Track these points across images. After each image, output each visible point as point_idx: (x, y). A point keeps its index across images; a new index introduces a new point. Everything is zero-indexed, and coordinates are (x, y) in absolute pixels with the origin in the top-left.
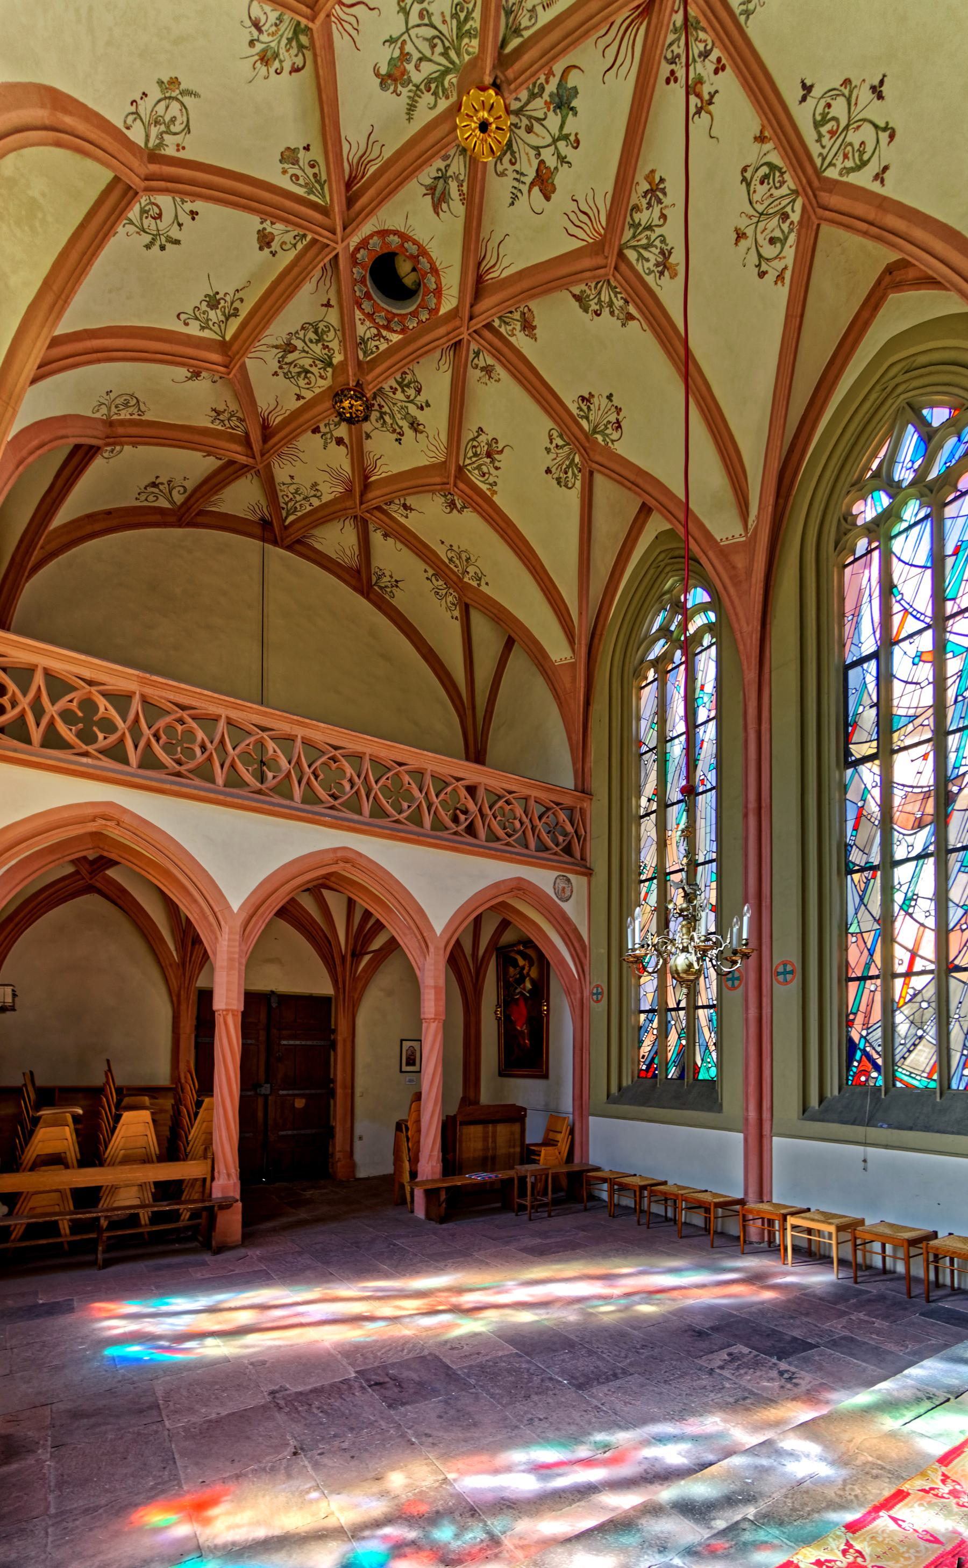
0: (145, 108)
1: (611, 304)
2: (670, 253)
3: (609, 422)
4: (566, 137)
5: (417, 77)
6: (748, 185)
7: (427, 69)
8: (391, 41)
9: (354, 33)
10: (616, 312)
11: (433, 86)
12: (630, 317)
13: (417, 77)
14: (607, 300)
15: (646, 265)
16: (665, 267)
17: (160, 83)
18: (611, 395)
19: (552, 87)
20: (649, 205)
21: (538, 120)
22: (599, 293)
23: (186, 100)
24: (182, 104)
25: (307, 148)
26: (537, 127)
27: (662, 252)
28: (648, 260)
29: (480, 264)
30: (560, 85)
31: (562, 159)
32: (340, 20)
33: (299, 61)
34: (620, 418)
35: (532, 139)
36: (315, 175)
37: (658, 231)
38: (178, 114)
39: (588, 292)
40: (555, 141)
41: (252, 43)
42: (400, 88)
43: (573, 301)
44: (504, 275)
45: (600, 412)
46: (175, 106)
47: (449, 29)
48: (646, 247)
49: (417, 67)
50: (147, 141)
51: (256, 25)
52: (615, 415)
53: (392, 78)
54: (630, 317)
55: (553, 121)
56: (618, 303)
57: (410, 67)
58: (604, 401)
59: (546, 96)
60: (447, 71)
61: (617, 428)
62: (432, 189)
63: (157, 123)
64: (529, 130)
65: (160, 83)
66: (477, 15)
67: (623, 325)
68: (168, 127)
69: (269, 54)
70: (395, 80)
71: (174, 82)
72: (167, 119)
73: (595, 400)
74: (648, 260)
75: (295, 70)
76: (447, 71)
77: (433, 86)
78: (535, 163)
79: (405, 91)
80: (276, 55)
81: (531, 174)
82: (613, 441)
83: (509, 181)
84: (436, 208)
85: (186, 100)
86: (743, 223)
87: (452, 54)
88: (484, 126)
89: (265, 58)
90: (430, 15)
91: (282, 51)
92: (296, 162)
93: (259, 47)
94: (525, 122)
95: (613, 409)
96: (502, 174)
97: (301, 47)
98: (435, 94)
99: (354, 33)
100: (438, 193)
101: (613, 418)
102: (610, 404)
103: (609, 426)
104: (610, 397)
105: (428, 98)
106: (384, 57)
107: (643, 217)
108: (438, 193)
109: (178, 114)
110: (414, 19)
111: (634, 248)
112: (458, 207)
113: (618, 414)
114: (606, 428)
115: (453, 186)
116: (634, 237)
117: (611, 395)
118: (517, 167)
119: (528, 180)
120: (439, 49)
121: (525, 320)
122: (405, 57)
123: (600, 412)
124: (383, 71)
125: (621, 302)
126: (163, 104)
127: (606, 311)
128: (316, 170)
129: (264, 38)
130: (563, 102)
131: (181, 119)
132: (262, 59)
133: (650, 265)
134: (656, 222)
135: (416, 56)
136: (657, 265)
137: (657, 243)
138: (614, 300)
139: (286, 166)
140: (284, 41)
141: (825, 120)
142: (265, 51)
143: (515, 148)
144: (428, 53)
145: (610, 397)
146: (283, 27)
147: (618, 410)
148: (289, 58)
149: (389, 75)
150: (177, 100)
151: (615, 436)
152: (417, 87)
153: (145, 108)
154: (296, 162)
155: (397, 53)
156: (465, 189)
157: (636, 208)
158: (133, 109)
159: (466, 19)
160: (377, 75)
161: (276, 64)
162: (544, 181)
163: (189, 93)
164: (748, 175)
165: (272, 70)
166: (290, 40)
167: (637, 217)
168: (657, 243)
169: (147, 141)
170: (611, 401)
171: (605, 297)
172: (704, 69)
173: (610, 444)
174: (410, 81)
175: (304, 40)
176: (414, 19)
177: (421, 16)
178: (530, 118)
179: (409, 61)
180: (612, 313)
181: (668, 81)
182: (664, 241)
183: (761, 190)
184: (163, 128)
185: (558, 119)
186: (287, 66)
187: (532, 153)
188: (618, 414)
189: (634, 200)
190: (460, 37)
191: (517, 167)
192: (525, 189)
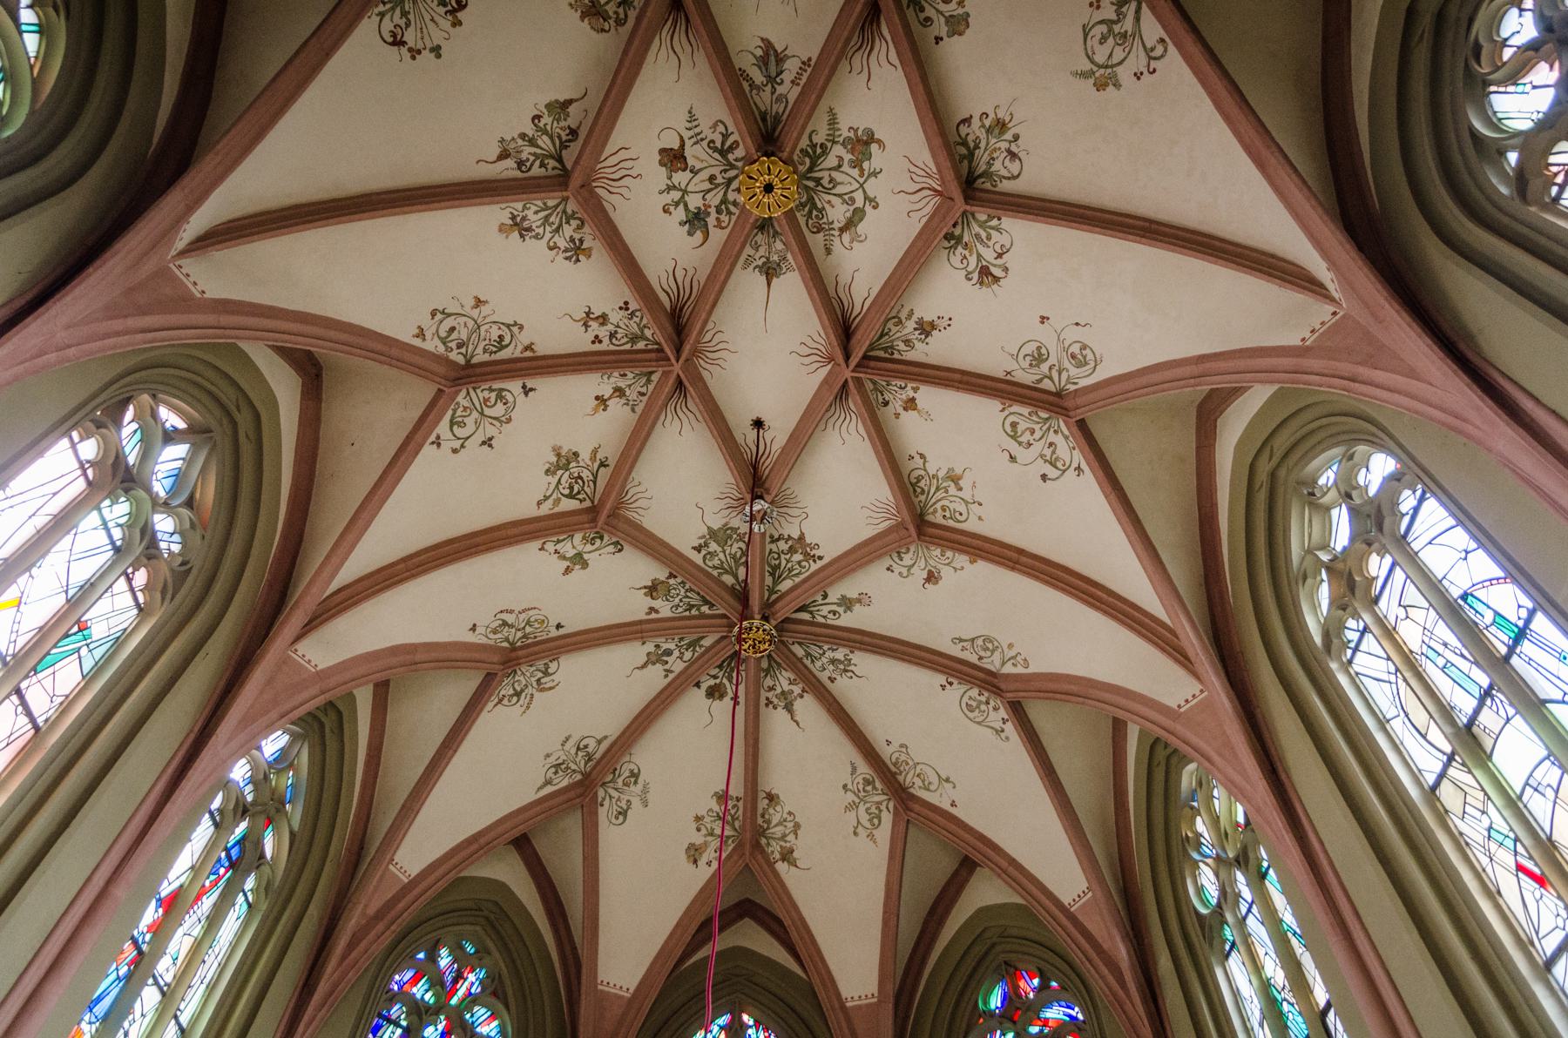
0: (1137, 60)
1: (532, 142)
2: (522, 236)
3: (408, 25)
4: (677, 204)
5: (838, 150)
6: (508, 326)
7: (831, 161)
8: (875, 174)
9: (913, 169)
10: (520, 142)
11: (819, 151)
12: (504, 155)
13: (838, 150)
14: (540, 142)
15: (534, 208)
16: (516, 224)
17: (1117, 85)
18: (439, 56)
19: (711, 221)
20: (572, 240)
21: (709, 191)
22: (551, 138)
23: (1088, 66)
24: (1092, 62)
25: (938, 39)
26: (707, 185)
27: (529, 229)
28: (536, 213)
29: (688, 21)
30: (706, 225)
31: (669, 188)
32: (930, 176)
33: (964, 130)
34: (404, 50)
35: (705, 175)
36: (922, 10)
37: (548, 236)
38: (1097, 47)
39: (563, 124)
40: (685, 192)
41: (1016, 138)
42: (852, 134)
43: (568, 97)
44: (657, 41)
45: (427, 18)
46: (1100, 58)
47: (822, 199)
48: (547, 218)
49: (841, 158)
50: (1138, 11)
51: (1013, 155)
52: (411, 44)
53: (863, 143)
54: (504, 155)
55: (694, 202)
56: (527, 152)
57: (847, 157)
58: (437, 37)
59: (713, 210)
60: (811, 170)
61: (394, 35)
62: (780, 60)
63: (1124, 35)
64: (712, 178)
65: (1117, 85)
66: (802, 221)
67: (502, 141)
68: (1110, 30)
69: (997, 131)
70: (858, 141)
71: (1100, 86)
72: (1111, 41)
73: (445, 24)
74: (536, 213)
75: (967, 121)
76: (811, 170)
77: (819, 151)
78: (691, 162)
79: (845, 133)
80: (989, 131)
81: (688, 152)
82: (382, 15)
83: (705, 126)
84: (768, 45)
85: (1088, 66)
86: (485, 310)
87: (811, 184)
88: (769, 188)
89: (1001, 126)
90: (845, 202)
91: (982, 134)
92: (950, 20)
93: (1008, 136)
94: (720, 180)
95: (420, 46)
96: (715, 126)
97: (964, 143)
98: (814, 146)
99: (913, 169)
100: (772, 58)
101: (410, 37)
102: (429, 45)
103: (402, 22)
104: (436, 50)
105: (818, 139)
106: (878, 158)
107: (568, 230)
108: (772, 58)
109: (1097, 47)
110: (859, 196)
111: (557, 206)
112: (745, 62)
113: (410, 50)
114: (404, 14)
115: (759, 78)
116: (564, 211)
117: (439, 56)
118: (705, 143)
119: (688, 143)
120: (825, 182)
121: (598, 14)
122: (857, 164)
123: (427, 18)
124: (874, 147)
125: (524, 156)
126: (1115, 60)
127: (530, 130)
128: (922, 16)
129: (1004, 145)
130: (696, 220)
131: (1093, 42)
132: (1004, 125)
133: (530, 213)
134: (556, 239)
135: (846, 168)
136: (524, 219)
137: (541, 230)
138: (533, 150)
139: (961, 11)
140: (983, 145)
141: (500, 397)
142: (1002, 132)
143: (716, 155)
144: (834, 174)
145: (436, 50)
146: (986, 158)
147: (415, 53)
148: (975, 130)
149: (867, 143)
150: (1100, 67)
151: (387, 25)
152: (834, 142)
153: (1137, 60)
154: (950, 20)
155: (866, 165)
156: (746, 85)
157: (579, 228)
158: (1153, 64)
159: (810, 212)
160: (879, 142)
161: (987, 123)
162: (674, 158)
163: (1084, 75)
164: (515, 329)
165: (992, 116)
166: (977, 147)
167: (574, 223)
168: (541, 230)
169: (1138, 11)
170: (432, 50)
171: (544, 142)
172: (603, 332)
173: (381, 8)
174: (843, 144)
175: (963, 151)
176: (859, 196)
177: (853, 200)
178: (717, 186)
179: (851, 161)
180: (523, 136)
181: (626, 303)
182: (537, 237)
183: (495, 333)
184: (1117, 28)
185: (692, 207)
186: (976, 122)
187: (698, 166)
188: (410, 50)
189: (587, 229)
190: (811, 200)
191: (705, 143)
192: (686, 134)
